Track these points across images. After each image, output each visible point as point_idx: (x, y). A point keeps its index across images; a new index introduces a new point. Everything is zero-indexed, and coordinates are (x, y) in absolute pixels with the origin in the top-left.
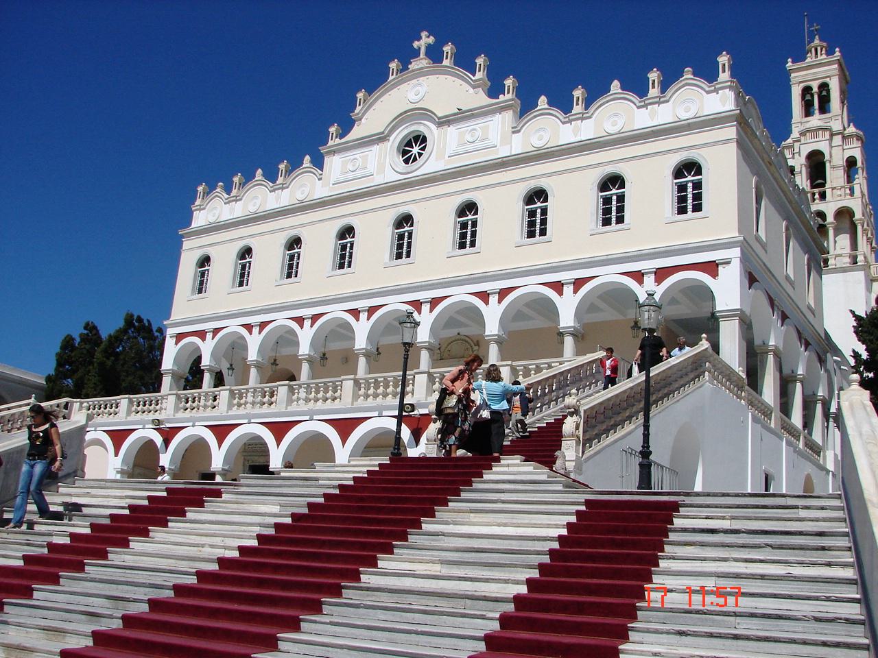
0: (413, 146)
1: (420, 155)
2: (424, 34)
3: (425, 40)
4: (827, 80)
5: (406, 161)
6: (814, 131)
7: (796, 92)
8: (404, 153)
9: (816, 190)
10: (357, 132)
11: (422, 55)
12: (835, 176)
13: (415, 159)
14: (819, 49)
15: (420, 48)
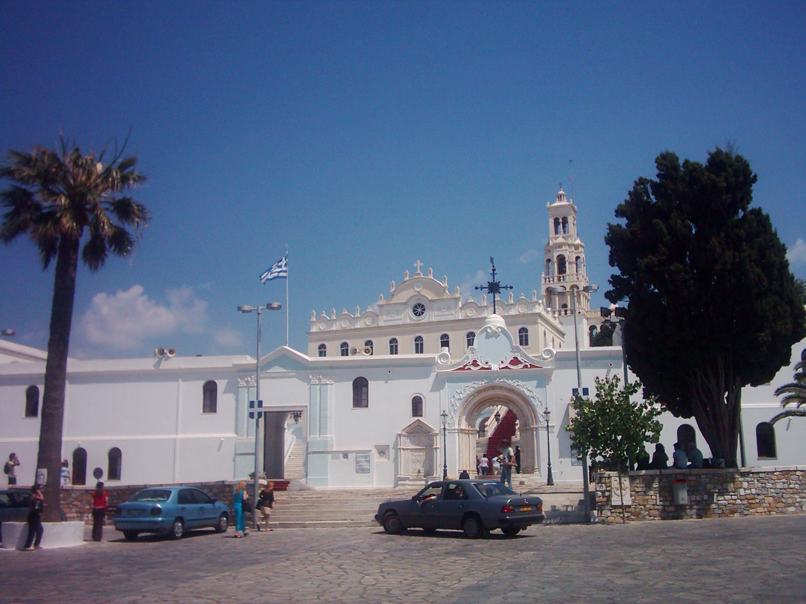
0: (419, 309)
1: (423, 313)
2: (418, 261)
3: (419, 264)
4: (566, 216)
5: (416, 314)
6: (560, 246)
7: (551, 221)
8: (414, 311)
9: (562, 275)
10: (395, 300)
11: (419, 272)
12: (570, 269)
13: (420, 315)
14: (562, 196)
15: (417, 266)
